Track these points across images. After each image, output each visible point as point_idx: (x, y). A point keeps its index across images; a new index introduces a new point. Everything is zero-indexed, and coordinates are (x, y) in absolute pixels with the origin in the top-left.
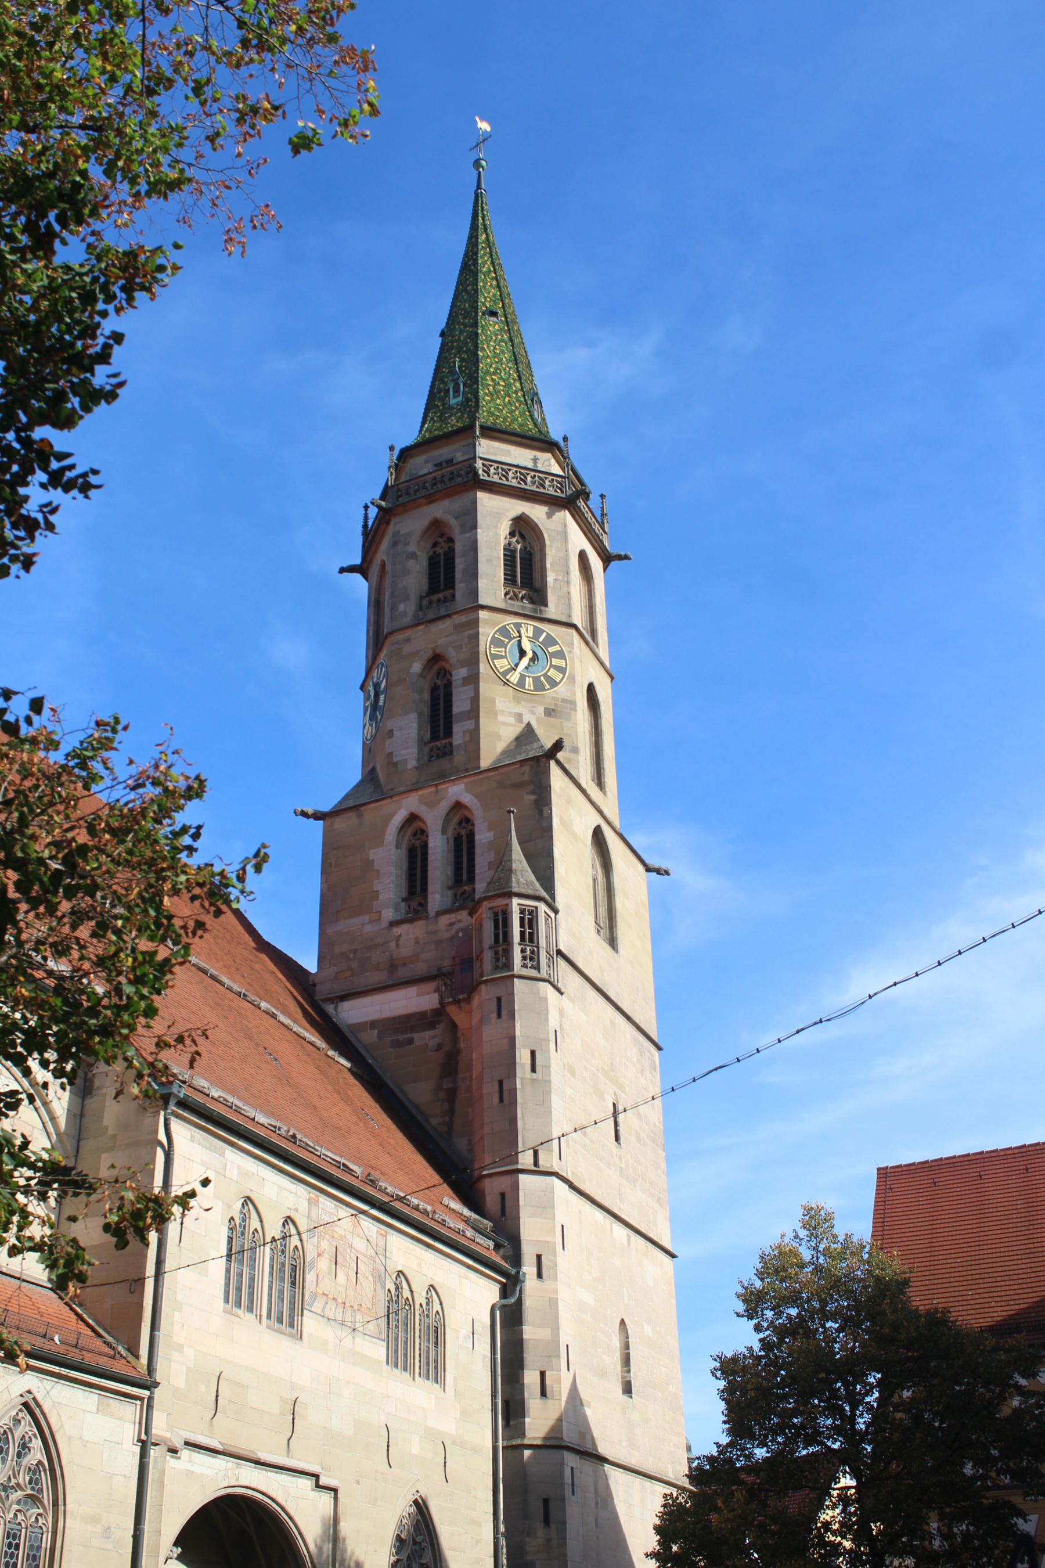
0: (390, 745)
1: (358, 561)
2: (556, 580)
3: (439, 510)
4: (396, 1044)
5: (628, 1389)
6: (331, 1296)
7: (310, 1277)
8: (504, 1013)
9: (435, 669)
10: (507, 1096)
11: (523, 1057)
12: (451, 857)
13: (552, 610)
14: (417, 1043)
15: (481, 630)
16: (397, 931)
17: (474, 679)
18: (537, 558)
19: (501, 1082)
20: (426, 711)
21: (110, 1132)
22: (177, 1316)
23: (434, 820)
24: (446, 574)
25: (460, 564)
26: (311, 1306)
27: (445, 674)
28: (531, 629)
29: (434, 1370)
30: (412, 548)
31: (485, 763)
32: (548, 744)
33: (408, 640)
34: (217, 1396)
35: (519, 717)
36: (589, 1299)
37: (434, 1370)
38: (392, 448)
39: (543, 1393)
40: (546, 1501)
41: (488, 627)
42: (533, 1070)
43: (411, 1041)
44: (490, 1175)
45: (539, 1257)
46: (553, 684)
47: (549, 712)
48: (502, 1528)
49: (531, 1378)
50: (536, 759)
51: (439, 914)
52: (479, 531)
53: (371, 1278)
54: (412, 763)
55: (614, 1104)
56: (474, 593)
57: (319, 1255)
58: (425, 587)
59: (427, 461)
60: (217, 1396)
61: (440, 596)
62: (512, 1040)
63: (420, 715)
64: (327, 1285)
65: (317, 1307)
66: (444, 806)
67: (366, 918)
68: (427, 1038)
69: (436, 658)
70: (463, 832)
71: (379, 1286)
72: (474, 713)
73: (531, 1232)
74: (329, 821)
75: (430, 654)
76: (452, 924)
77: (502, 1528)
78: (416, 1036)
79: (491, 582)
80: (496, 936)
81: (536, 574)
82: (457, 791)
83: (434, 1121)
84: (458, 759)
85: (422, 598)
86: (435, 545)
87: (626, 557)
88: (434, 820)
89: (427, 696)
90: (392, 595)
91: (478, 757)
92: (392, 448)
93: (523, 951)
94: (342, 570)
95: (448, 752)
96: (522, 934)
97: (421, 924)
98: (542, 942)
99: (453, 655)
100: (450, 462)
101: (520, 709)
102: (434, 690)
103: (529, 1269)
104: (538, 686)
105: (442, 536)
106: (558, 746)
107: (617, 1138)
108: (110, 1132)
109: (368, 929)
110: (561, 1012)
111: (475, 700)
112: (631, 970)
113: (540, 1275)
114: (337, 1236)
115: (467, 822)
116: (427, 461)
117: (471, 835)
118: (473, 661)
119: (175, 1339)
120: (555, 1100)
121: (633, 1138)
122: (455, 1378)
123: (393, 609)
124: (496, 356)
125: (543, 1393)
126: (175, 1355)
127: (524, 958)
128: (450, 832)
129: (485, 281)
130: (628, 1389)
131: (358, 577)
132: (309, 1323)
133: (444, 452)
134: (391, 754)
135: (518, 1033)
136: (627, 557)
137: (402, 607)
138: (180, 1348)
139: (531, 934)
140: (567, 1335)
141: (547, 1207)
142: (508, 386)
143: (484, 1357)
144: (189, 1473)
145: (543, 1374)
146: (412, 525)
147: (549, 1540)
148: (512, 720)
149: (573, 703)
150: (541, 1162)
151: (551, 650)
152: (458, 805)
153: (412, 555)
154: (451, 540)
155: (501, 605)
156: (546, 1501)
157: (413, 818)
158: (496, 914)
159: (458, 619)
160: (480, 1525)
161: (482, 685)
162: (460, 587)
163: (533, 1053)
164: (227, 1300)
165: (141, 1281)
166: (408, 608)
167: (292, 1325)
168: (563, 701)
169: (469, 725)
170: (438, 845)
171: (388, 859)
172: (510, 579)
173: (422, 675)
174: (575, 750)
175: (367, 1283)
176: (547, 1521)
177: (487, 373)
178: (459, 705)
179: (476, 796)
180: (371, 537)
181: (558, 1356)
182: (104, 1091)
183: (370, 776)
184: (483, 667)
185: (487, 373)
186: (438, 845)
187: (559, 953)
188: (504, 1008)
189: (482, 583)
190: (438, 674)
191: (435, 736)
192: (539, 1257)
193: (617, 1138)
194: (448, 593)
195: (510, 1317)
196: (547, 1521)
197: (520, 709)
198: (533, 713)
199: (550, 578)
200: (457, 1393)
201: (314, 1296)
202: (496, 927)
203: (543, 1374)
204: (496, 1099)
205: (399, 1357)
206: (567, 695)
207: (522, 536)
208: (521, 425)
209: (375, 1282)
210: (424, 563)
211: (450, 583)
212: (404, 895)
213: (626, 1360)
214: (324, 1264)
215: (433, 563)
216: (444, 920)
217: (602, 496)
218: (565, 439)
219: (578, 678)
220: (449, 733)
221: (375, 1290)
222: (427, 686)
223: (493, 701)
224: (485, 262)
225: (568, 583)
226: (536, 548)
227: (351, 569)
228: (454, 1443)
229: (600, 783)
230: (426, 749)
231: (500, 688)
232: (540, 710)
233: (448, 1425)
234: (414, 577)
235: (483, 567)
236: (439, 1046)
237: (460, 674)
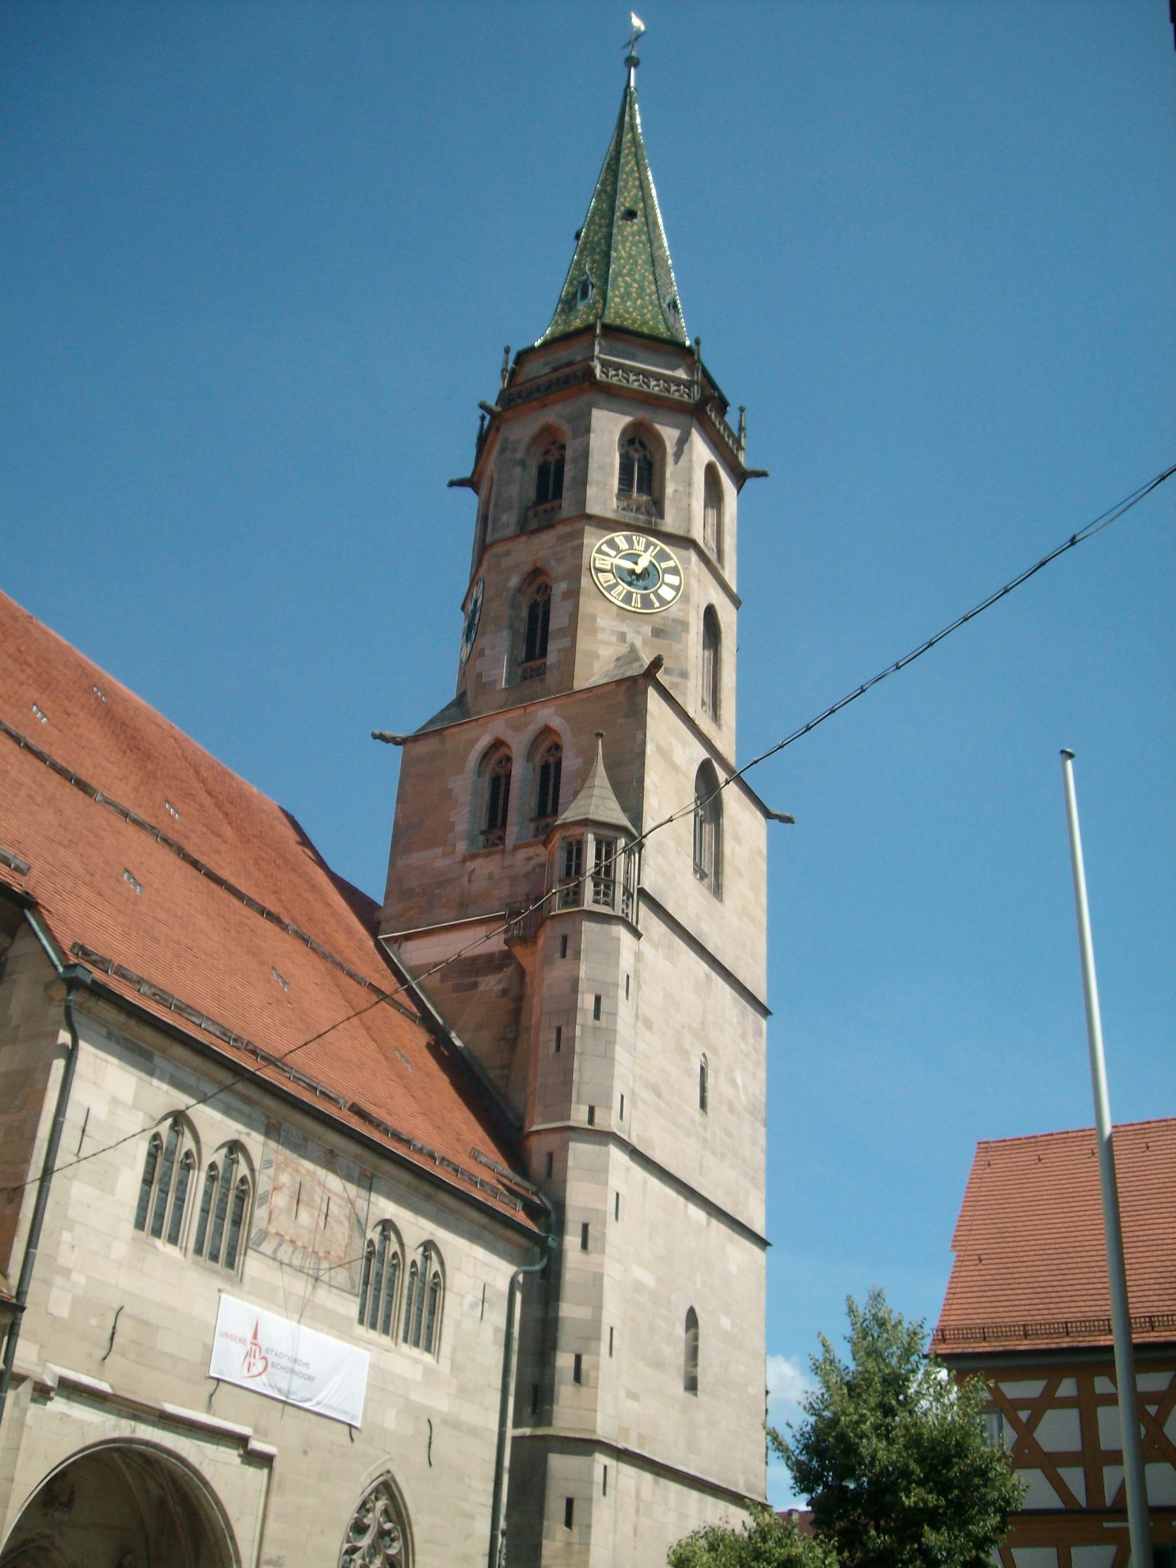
1: (467, 473)
2: (676, 491)
3: (553, 415)
4: (458, 988)
5: (692, 1385)
6: (287, 1238)
7: (261, 1213)
8: (568, 952)
10: (563, 1044)
11: (586, 1001)
12: (536, 786)
13: (670, 523)
14: (482, 988)
15: (586, 541)
16: (470, 865)
17: (574, 594)
18: (656, 468)
19: (559, 1030)
20: (523, 628)
21: (14, 1023)
22: (66, 1236)
23: (518, 745)
25: (569, 472)
26: (259, 1244)
27: (546, 589)
29: (424, 1332)
31: (579, 684)
32: (647, 661)
33: (508, 553)
34: (113, 1334)
35: (622, 637)
36: (649, 1280)
37: (424, 1332)
38: (507, 351)
39: (578, 1377)
40: (570, 1503)
42: (597, 1016)
43: (475, 986)
44: (538, 1132)
45: (585, 1227)
48: (502, 1524)
49: (564, 1361)
50: (633, 680)
51: (515, 848)
52: (592, 435)
53: (346, 1223)
55: (702, 1069)
57: (275, 1189)
58: (532, 493)
60: (113, 1334)
62: (575, 983)
63: (515, 634)
64: (282, 1224)
65: (268, 1247)
67: (440, 850)
68: (491, 984)
69: (537, 573)
70: (551, 760)
71: (356, 1234)
73: (579, 1196)
74: (409, 746)
75: (529, 568)
76: (529, 859)
77: (502, 1524)
78: (480, 979)
79: (603, 490)
80: (569, 868)
82: (547, 714)
83: (492, 1074)
84: (551, 678)
85: (527, 509)
86: (547, 452)
87: (764, 474)
88: (518, 745)
89: (525, 613)
90: (496, 506)
91: (571, 677)
92: (507, 351)
93: (596, 885)
94: (452, 484)
95: (540, 672)
97: (497, 858)
98: (620, 877)
100: (570, 364)
102: (533, 607)
103: (572, 1240)
105: (554, 443)
106: (657, 663)
107: (703, 1104)
108: (14, 1023)
109: (441, 863)
110: (638, 956)
111: (574, 616)
112: (739, 923)
113: (584, 1245)
114: (303, 1171)
117: (558, 764)
118: (575, 574)
119: (61, 1261)
120: (620, 1054)
121: (725, 1108)
122: (454, 1349)
123: (496, 520)
124: (630, 256)
125: (578, 1377)
126: (59, 1280)
127: (597, 893)
128: (538, 761)
129: (626, 182)
130: (692, 1385)
131: (468, 492)
132: (253, 1265)
133: (564, 354)
134: (480, 675)
135: (582, 975)
136: (764, 474)
137: (505, 517)
138: (67, 1273)
139: (608, 868)
140: (612, 1313)
141: (600, 1173)
142: (642, 289)
143: (496, 1329)
144: (63, 1417)
145: (578, 1359)
146: (522, 431)
147: (569, 1544)
148: (614, 639)
149: (684, 625)
150: (597, 1120)
151: (664, 565)
152: (547, 730)
155: (610, 515)
156: (570, 1503)
157: (498, 744)
158: (570, 844)
159: (561, 530)
160: (472, 1517)
161: (582, 599)
163: (598, 999)
164: (140, 1224)
165: (17, 1193)
166: (509, 519)
167: (230, 1264)
168: (675, 621)
169: (565, 642)
170: (521, 774)
171: (465, 788)
173: (519, 590)
174: (684, 675)
175: (341, 1232)
176: (569, 1523)
177: (620, 274)
179: (566, 719)
181: (598, 1339)
182: (15, 976)
184: (585, 582)
185: (620, 274)
186: (521, 774)
187: (642, 893)
188: (567, 947)
190: (538, 590)
191: (530, 656)
192: (585, 1227)
193: (703, 1104)
194: (556, 503)
195: (542, 1288)
196: (569, 1523)
197: (625, 629)
198: (639, 633)
199: (670, 489)
200: (455, 1367)
201: (264, 1235)
202: (569, 859)
203: (578, 1359)
204: (553, 1046)
205: (375, 1316)
206: (680, 615)
207: (642, 444)
208: (651, 328)
209: (351, 1229)
210: (534, 472)
211: (558, 494)
212: (484, 827)
213: (693, 1353)
214: (280, 1200)
215: (543, 471)
216: (522, 854)
217: (742, 410)
219: (694, 598)
220: (544, 653)
221: (350, 1237)
223: (594, 618)
224: (628, 163)
225: (690, 495)
226: (657, 457)
227: (461, 483)
228: (444, 1422)
229: (716, 717)
230: (519, 671)
231: (603, 604)
232: (647, 630)
233: (441, 1403)
234: (519, 485)
236: (505, 992)
237: (559, 588)
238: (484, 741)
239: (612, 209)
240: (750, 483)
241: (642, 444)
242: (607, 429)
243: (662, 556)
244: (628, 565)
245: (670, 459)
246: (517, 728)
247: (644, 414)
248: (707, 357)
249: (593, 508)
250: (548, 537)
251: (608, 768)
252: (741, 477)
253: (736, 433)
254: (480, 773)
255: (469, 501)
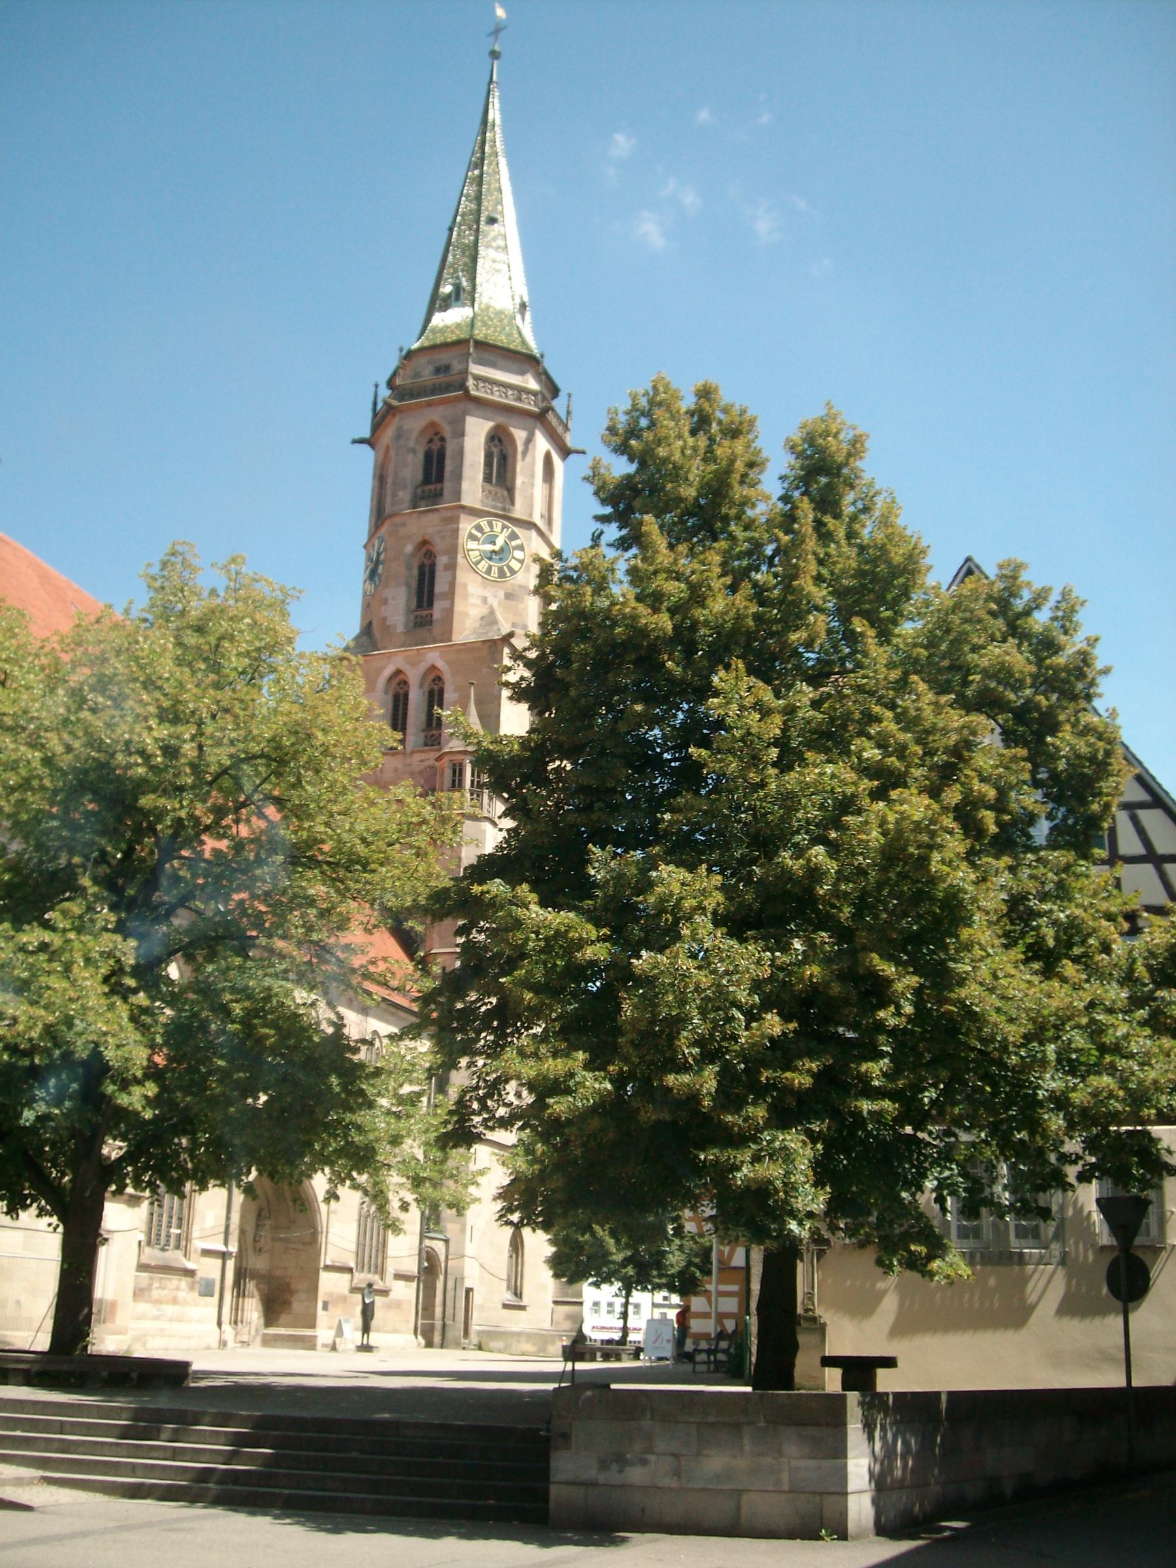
0: (386, 611)
2: (523, 482)
3: (435, 415)
9: (424, 550)
13: (518, 511)
15: (461, 526)
17: (452, 567)
18: (510, 460)
24: (437, 470)
27: (430, 555)
28: (500, 525)
30: (411, 444)
32: (504, 632)
33: (404, 525)
38: (401, 350)
41: (466, 525)
46: (513, 572)
47: (509, 596)
50: (493, 642)
51: (413, 752)
52: (466, 439)
54: (400, 628)
56: (457, 494)
58: (420, 476)
59: (429, 363)
61: (432, 487)
66: (423, 667)
69: (425, 542)
70: (436, 688)
72: (450, 595)
75: (420, 539)
76: (422, 761)
79: (473, 486)
80: (454, 781)
81: (509, 476)
82: (433, 655)
84: (437, 629)
85: (417, 487)
86: (431, 441)
88: (414, 677)
89: (415, 572)
90: (394, 483)
94: (354, 442)
96: (472, 781)
99: (439, 545)
101: (486, 593)
102: (421, 567)
104: (502, 574)
115: (439, 679)
116: (429, 363)
118: (453, 551)
123: (394, 495)
128: (426, 688)
129: (489, 184)
131: (366, 448)
133: (443, 357)
134: (384, 619)
135: (463, 855)
137: (401, 494)
146: (415, 423)
148: (479, 602)
151: (514, 543)
152: (433, 667)
153: (413, 451)
154: (443, 439)
155: (478, 506)
157: (398, 672)
158: (455, 765)
161: (458, 573)
162: (448, 485)
166: (405, 495)
168: (521, 587)
169: (446, 604)
170: (416, 698)
172: (488, 478)
173: (413, 555)
178: (440, 587)
179: (448, 663)
180: (380, 419)
183: (367, 630)
184: (460, 560)
186: (416, 698)
189: (465, 485)
190: (425, 554)
191: (420, 605)
194: (438, 486)
197: (486, 593)
198: (495, 596)
199: (519, 481)
202: (454, 775)
207: (500, 441)
210: (421, 456)
211: (440, 478)
215: (428, 456)
217: (570, 396)
218: (542, 356)
220: (430, 604)
222: (416, 564)
223: (466, 586)
225: (533, 485)
227: (362, 441)
230: (412, 617)
232: (501, 594)
234: (412, 469)
235: (467, 472)
237: (442, 560)
238: (389, 671)
239: (479, 212)
240: (572, 457)
241: (500, 441)
242: (476, 432)
243: (513, 536)
244: (490, 547)
245: (519, 456)
246: (413, 664)
247: (502, 419)
248: (548, 364)
249: (466, 501)
250: (434, 518)
251: (476, 704)
252: (565, 452)
253: (563, 417)
254: (386, 692)
255: (367, 457)
